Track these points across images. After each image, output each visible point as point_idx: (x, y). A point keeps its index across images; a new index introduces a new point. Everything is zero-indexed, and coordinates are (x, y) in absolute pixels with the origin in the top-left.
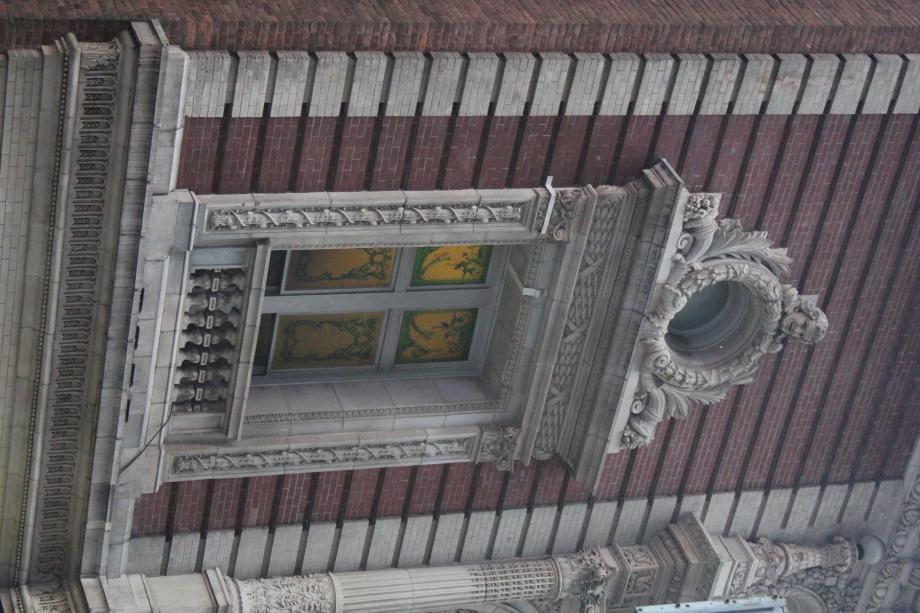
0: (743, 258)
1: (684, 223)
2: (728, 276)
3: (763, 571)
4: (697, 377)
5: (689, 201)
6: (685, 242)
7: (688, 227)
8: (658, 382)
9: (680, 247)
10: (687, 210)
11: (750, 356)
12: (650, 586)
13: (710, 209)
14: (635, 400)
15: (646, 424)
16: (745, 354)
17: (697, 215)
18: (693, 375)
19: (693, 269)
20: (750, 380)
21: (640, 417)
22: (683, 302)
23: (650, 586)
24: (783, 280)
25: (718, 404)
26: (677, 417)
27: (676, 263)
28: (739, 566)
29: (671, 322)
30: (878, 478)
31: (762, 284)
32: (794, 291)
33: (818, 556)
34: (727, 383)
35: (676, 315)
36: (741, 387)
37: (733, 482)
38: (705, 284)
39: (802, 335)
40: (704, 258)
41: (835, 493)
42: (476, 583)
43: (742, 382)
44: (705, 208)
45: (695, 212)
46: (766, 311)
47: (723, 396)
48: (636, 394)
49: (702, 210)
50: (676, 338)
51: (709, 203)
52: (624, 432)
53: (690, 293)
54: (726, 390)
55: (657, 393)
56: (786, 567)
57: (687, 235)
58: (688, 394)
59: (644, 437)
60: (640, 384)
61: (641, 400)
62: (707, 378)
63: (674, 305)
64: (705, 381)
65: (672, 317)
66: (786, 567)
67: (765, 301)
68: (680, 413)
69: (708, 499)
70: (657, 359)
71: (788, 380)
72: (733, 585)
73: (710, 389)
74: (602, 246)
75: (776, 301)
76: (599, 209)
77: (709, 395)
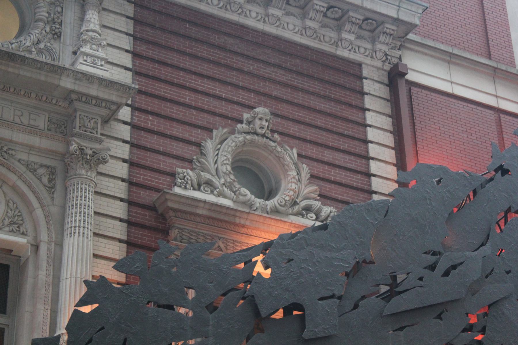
0: (217, 155)
1: (194, 189)
2: (228, 164)
3: (94, 46)
4: (291, 182)
5: (180, 187)
6: (206, 189)
7: (196, 187)
8: (295, 203)
9: (209, 192)
10: (185, 188)
11: (278, 152)
12: (92, 118)
13: (185, 174)
14: (307, 218)
15: (323, 211)
16: (278, 155)
17: (189, 182)
18: (290, 185)
19: (224, 184)
20: (295, 151)
21: (317, 215)
22: (244, 190)
23: (92, 118)
24: (232, 132)
25: (309, 169)
26: (318, 193)
27: (221, 194)
28: (86, 61)
29: (256, 197)
30: (361, 78)
31: (234, 144)
32: (239, 126)
33: (90, 12)
34: (295, 164)
35: (252, 193)
36: (299, 155)
37: (363, 161)
38: (232, 177)
39: (266, 121)
40: (217, 177)
41: (368, 102)
42: (77, 234)
43: (296, 156)
44: (185, 177)
45: (187, 183)
46: (250, 143)
47: (305, 166)
48: (303, 217)
49: (186, 179)
50: (270, 195)
51: (181, 175)
52: (182, 188)
53: (238, 186)
54: (300, 164)
55: (303, 204)
56: (94, 31)
57: (202, 188)
58: (303, 187)
59: (331, 212)
60: (297, 214)
61: (307, 215)
62: (292, 176)
63: (245, 195)
64: (294, 178)
65: (253, 197)
66: (94, 31)
67: (244, 143)
68: (316, 191)
69: (374, 175)
70: (281, 206)
71: (294, 129)
72: (102, 65)
73: (299, 174)
74: (191, 235)
75: (245, 137)
76: (183, 241)
77: (303, 175)
